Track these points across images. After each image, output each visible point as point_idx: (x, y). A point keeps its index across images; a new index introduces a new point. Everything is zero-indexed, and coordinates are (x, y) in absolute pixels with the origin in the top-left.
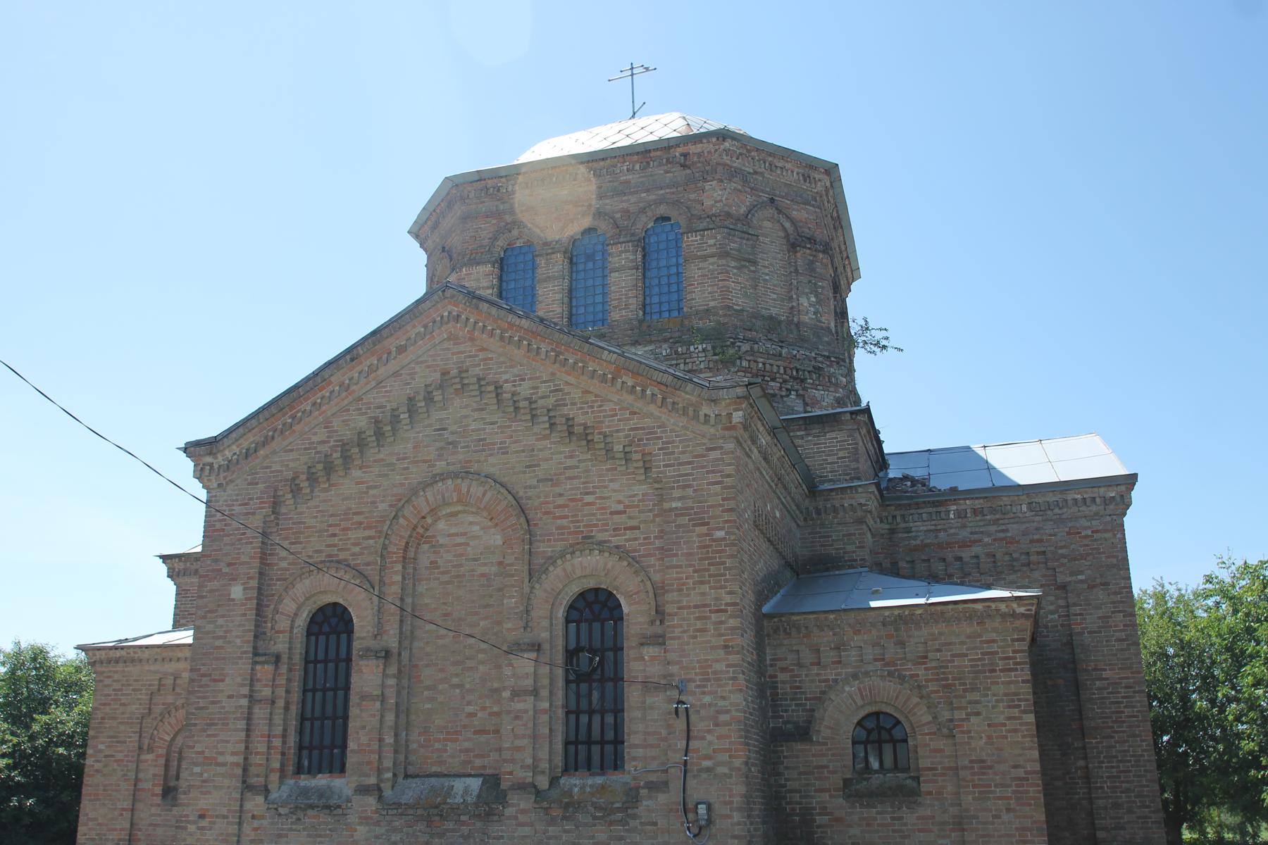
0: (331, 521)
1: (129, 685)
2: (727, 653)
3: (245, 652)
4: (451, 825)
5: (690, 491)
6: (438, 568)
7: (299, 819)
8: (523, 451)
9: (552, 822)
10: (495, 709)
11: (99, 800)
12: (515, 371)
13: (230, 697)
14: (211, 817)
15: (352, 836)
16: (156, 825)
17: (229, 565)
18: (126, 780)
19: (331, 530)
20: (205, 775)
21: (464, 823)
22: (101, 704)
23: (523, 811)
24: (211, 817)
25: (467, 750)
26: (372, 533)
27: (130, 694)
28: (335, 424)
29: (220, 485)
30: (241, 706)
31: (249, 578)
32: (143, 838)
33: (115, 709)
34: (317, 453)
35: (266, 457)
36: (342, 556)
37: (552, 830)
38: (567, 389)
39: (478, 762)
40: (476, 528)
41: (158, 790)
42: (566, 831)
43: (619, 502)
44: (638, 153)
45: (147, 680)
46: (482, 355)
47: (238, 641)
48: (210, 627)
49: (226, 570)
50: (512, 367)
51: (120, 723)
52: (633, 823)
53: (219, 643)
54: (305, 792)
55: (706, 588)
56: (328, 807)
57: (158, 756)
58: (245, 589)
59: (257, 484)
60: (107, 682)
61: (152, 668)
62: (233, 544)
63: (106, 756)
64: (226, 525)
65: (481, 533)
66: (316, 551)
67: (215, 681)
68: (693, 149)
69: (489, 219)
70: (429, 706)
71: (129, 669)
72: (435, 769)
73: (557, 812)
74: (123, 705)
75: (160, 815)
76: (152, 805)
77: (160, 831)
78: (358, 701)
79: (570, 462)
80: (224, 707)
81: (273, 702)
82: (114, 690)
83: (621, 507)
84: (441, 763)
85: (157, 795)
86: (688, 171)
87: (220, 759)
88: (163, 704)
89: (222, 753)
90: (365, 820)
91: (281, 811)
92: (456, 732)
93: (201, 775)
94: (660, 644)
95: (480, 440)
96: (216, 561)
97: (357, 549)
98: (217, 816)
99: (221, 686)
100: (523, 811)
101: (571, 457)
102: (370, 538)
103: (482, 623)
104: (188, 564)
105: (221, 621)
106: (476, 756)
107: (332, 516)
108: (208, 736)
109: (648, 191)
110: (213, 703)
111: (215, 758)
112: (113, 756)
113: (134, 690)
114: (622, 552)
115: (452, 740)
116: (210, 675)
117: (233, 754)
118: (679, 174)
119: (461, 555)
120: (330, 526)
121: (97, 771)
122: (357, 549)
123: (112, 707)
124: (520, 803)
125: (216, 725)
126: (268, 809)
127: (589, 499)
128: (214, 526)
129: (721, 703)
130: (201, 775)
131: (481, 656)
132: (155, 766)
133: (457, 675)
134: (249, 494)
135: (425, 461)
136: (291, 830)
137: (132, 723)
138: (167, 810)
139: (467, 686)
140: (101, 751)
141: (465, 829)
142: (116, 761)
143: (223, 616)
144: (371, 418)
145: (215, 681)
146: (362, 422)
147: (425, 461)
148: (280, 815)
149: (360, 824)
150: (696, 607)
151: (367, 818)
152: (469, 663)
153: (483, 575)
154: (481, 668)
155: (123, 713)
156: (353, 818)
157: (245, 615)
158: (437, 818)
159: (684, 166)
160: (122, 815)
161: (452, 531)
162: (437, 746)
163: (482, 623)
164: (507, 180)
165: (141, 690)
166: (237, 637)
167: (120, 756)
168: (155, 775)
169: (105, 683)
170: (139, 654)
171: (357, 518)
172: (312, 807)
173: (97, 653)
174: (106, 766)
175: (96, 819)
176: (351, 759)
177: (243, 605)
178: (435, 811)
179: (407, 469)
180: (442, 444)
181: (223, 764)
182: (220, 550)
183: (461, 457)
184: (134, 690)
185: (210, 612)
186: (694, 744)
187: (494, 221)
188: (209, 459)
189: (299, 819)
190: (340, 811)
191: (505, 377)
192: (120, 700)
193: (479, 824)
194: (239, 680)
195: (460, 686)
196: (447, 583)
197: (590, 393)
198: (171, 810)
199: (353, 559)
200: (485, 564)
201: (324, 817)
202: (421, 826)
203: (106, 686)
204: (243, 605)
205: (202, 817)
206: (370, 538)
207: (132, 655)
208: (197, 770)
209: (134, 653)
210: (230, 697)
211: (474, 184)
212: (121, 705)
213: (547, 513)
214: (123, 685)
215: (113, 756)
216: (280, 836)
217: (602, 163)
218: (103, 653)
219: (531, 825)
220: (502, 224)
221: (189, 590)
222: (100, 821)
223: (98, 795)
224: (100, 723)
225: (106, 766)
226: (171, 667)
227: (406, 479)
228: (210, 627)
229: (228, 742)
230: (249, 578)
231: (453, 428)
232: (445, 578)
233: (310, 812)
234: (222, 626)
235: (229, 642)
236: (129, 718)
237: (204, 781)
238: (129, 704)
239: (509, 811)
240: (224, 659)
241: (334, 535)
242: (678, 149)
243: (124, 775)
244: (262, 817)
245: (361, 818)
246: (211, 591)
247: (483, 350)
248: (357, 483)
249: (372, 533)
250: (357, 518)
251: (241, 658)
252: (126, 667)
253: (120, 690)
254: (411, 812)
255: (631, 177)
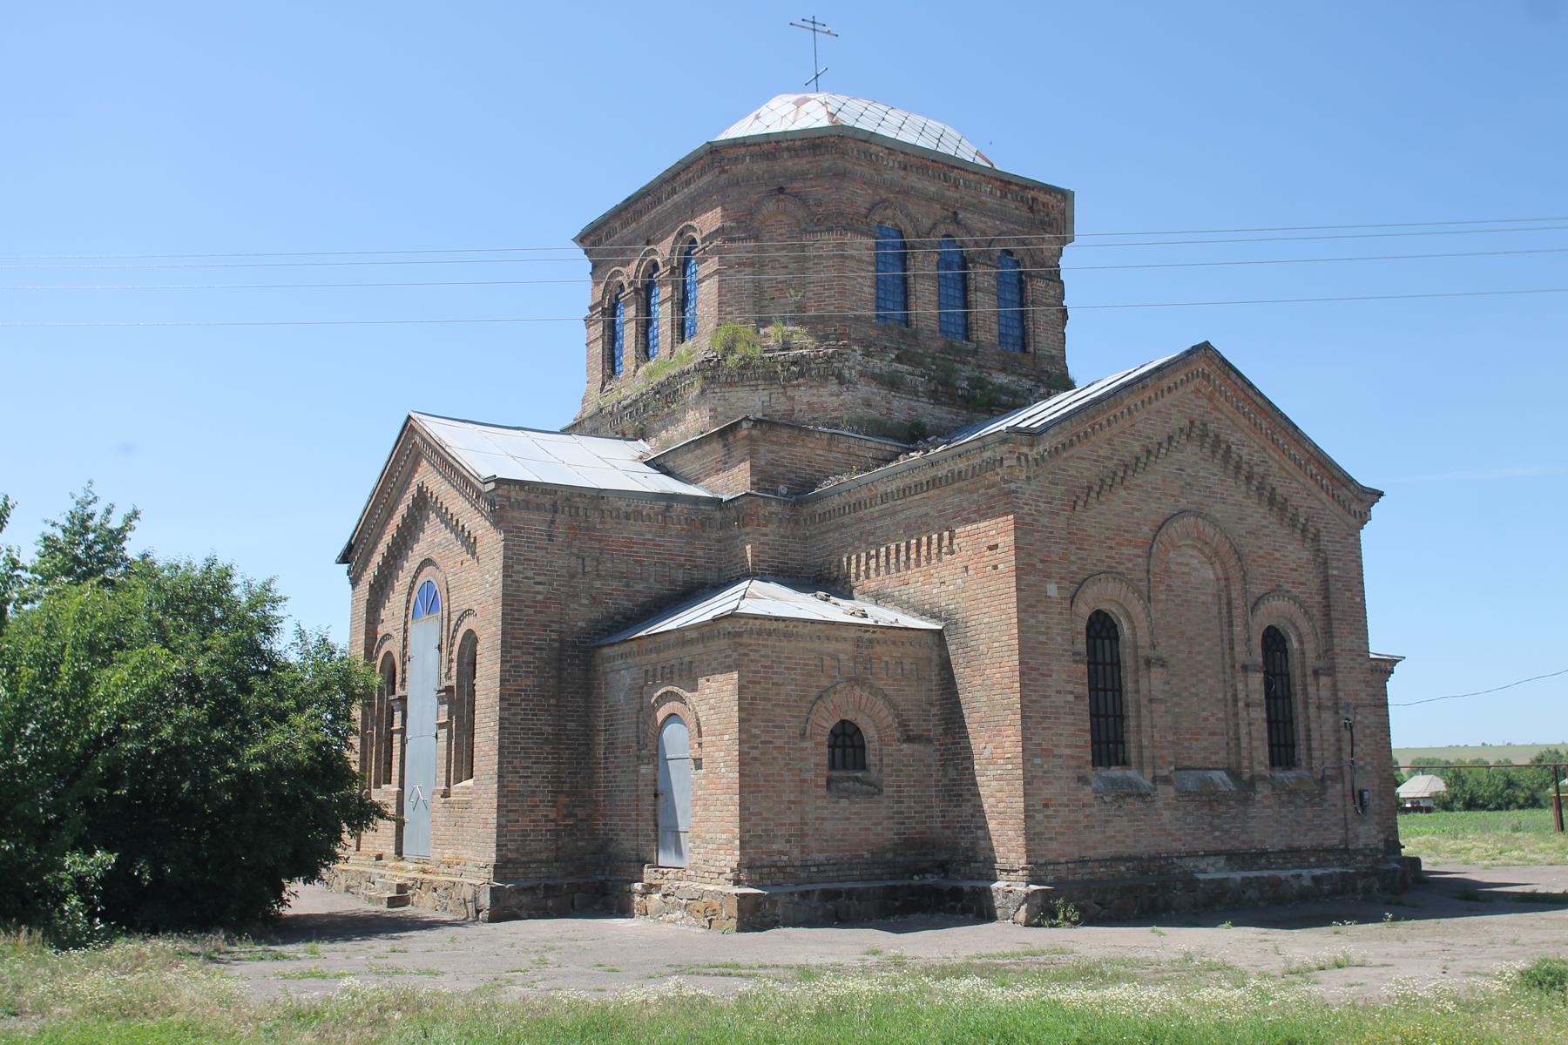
0: (1108, 533)
1: (781, 663)
2: (1366, 686)
3: (1066, 650)
4: (1222, 808)
5: (1341, 564)
6: (1172, 591)
7: (1120, 806)
8: (1235, 505)
9: (1282, 805)
10: (1221, 715)
11: (761, 791)
12: (1238, 435)
13: (1058, 692)
14: (1054, 805)
15: (1160, 820)
16: (823, 819)
17: (1042, 561)
18: (789, 770)
19: (1109, 543)
20: (1046, 766)
21: (1232, 807)
22: (748, 682)
23: (1266, 797)
24: (1054, 805)
25: (1205, 748)
26: (1139, 551)
27: (781, 673)
28: (1115, 443)
29: (1028, 478)
30: (1068, 702)
31: (1061, 578)
32: (810, 833)
33: (766, 689)
34: (1105, 467)
35: (1066, 459)
36: (1121, 569)
37: (1284, 810)
38: (1271, 462)
39: (1214, 758)
40: (1196, 561)
41: (822, 781)
42: (1291, 812)
43: (1294, 562)
44: (1002, 181)
45: (801, 659)
46: (1215, 414)
47: (1059, 639)
48: (1032, 621)
49: (1040, 566)
50: (1236, 431)
51: (775, 705)
52: (1326, 805)
53: (1042, 638)
54: (1113, 782)
55: (1353, 637)
56: (1140, 795)
57: (817, 744)
58: (1059, 588)
59: (1057, 484)
60: (753, 656)
61: (809, 645)
62: (1042, 541)
63: (762, 742)
64: (1034, 520)
65: (1199, 566)
66: (1099, 560)
67: (1043, 675)
68: (1043, 197)
69: (865, 187)
70: (1177, 710)
71: (781, 644)
72: (1187, 763)
73: (1284, 798)
74: (777, 684)
75: (827, 808)
76: (816, 797)
77: (828, 825)
78: (1146, 702)
79: (1265, 522)
80: (1053, 702)
81: (1247, 705)
82: (763, 666)
83: (1294, 566)
84: (1190, 758)
85: (821, 786)
86: (1031, 215)
87: (1057, 751)
88: (817, 687)
89: (1057, 746)
90: (1168, 806)
91: (1106, 799)
92: (1198, 734)
93: (1042, 766)
94: (1329, 675)
95: (1208, 487)
96: (1030, 555)
97: (1130, 565)
98: (1060, 805)
99: (1050, 681)
100: (1266, 797)
101: (1264, 518)
102: (1139, 556)
103: (1206, 644)
104: (532, 495)
105: (1041, 617)
106: (1211, 753)
107: (1108, 529)
108: (1044, 728)
109: (1002, 220)
110: (1045, 697)
111: (1051, 751)
112: (771, 742)
113: (786, 668)
114: (1295, 599)
115: (1197, 740)
116: (1038, 669)
117: (1067, 746)
118: (1024, 212)
119: (1187, 583)
120: (1107, 538)
121: (755, 759)
122: (1130, 565)
123: (763, 685)
124: (1263, 790)
125: (1050, 718)
126: (1096, 797)
127: (1277, 555)
128: (1024, 519)
129: (1366, 722)
130: (1042, 766)
131: (1208, 671)
132: (816, 755)
133: (1194, 686)
134: (1051, 493)
135: (1172, 496)
136: (1115, 816)
137: (788, 706)
138: (833, 802)
139: (1202, 695)
140: (756, 736)
141: (1233, 812)
142: (775, 748)
143: (1043, 612)
144: (1143, 446)
145: (1043, 675)
146: (1137, 448)
147: (1172, 496)
148: (1106, 803)
149: (1165, 809)
150: (1350, 650)
151: (1169, 804)
152: (1202, 677)
153: (1203, 603)
154: (1210, 682)
155: (778, 694)
156: (1159, 804)
157: (1061, 614)
158: (1215, 803)
159: (1031, 209)
160: (790, 808)
161: (1179, 560)
162: (1186, 744)
163: (1206, 644)
164: (889, 154)
165: (795, 669)
166: (1058, 634)
167: (779, 743)
168: (816, 765)
169: (752, 658)
170: (801, 629)
171: (1128, 536)
172: (1129, 795)
173: (751, 622)
174: (764, 753)
175: (760, 814)
176: (1133, 755)
177: (1059, 603)
178: (1213, 798)
179: (1159, 499)
180: (1182, 483)
181: (1061, 756)
182: (1032, 545)
183: (1196, 498)
184: (786, 668)
185: (1031, 606)
186: (1355, 749)
187: (870, 191)
188: (1025, 450)
189: (1120, 806)
190: (1149, 799)
191: (1232, 439)
192: (772, 678)
193: (1241, 808)
194: (1064, 676)
195: (1196, 695)
196: (1178, 605)
197: (1285, 470)
198: (837, 803)
199: (1129, 574)
200: (1204, 594)
201: (1138, 805)
202: (1205, 810)
203: (752, 661)
204: (1059, 603)
205: (1046, 806)
206: (1139, 556)
207: (791, 628)
208: (1038, 761)
209: (794, 626)
210: (1058, 692)
211: (859, 143)
212: (773, 684)
213: (1254, 561)
214: (773, 662)
215: (771, 742)
216: (1107, 821)
217: (971, 176)
218: (758, 622)
219: (1271, 807)
220: (878, 198)
221: (523, 528)
222: (765, 815)
223: (758, 786)
224: (750, 704)
225: (764, 753)
226: (831, 647)
227: (1160, 508)
228: (1032, 621)
229: (1061, 735)
230: (1061, 578)
231: (1189, 471)
232: (1178, 601)
233: (1129, 800)
234: (1042, 622)
235: (1052, 639)
236: (783, 700)
237: (1045, 772)
238: (783, 684)
239: (1258, 797)
240: (1048, 654)
241: (1111, 548)
242: (1032, 192)
243: (787, 764)
244: (1091, 805)
245: (1165, 804)
246: (1028, 585)
247: (1216, 408)
248: (1124, 503)
249: (1139, 551)
250: (1128, 536)
251: (1063, 655)
252: (780, 641)
253: (771, 667)
254: (1198, 798)
255: (989, 200)
